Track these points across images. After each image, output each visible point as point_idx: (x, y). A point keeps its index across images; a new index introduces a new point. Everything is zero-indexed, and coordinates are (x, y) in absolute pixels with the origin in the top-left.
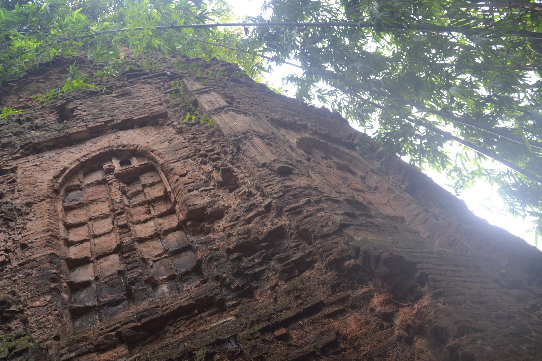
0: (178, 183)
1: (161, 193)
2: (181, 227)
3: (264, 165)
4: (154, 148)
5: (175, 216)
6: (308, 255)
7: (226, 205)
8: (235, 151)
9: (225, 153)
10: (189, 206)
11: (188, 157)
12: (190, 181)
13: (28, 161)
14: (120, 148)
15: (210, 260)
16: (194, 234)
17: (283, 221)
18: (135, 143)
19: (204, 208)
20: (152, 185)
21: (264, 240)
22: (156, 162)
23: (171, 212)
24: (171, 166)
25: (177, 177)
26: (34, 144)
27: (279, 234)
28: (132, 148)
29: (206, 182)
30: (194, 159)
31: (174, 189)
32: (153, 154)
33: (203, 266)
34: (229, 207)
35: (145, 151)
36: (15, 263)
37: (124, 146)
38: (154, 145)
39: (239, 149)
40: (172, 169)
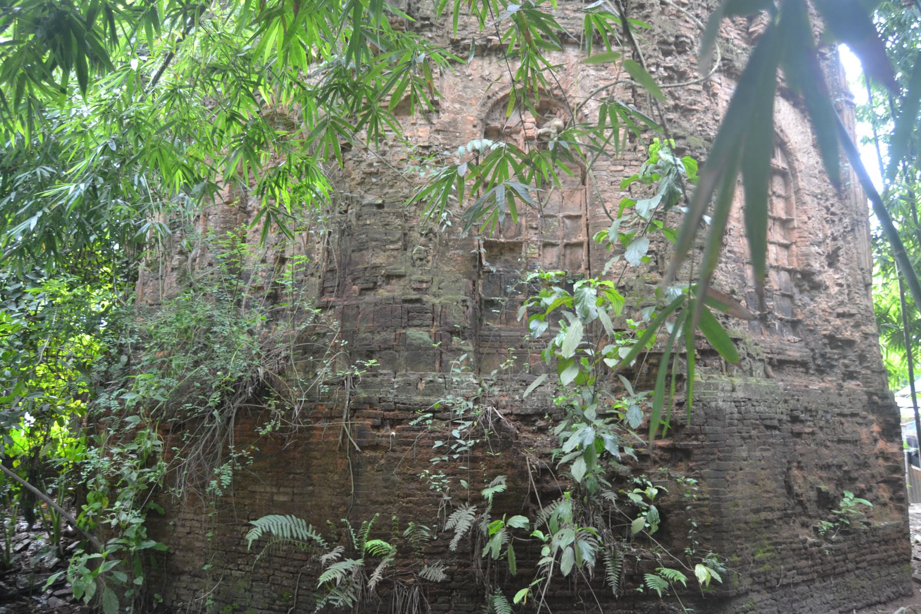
0: (805, 227)
1: (784, 217)
2: (789, 271)
3: (862, 269)
4: (799, 155)
5: (786, 253)
6: (856, 372)
7: (827, 283)
8: (849, 229)
9: (840, 220)
10: (809, 265)
11: (816, 197)
12: (812, 231)
13: (720, 84)
14: (778, 131)
15: (811, 331)
16: (797, 285)
17: (857, 336)
18: (788, 132)
19: (814, 274)
20: (779, 196)
21: (841, 340)
22: (795, 176)
23: (786, 247)
24: (808, 199)
25: (805, 218)
26: (734, 66)
27: (850, 343)
28: (786, 140)
29: (820, 242)
30: (819, 204)
31: (799, 228)
32: (796, 164)
33: (801, 326)
34: (827, 288)
35: (791, 154)
36: (727, 248)
37: (782, 131)
38: (799, 150)
39: (853, 230)
40: (804, 203)
